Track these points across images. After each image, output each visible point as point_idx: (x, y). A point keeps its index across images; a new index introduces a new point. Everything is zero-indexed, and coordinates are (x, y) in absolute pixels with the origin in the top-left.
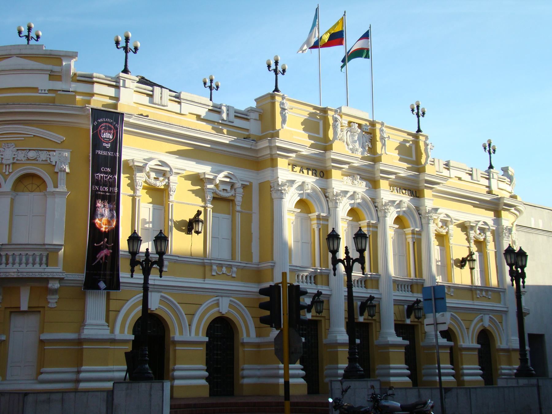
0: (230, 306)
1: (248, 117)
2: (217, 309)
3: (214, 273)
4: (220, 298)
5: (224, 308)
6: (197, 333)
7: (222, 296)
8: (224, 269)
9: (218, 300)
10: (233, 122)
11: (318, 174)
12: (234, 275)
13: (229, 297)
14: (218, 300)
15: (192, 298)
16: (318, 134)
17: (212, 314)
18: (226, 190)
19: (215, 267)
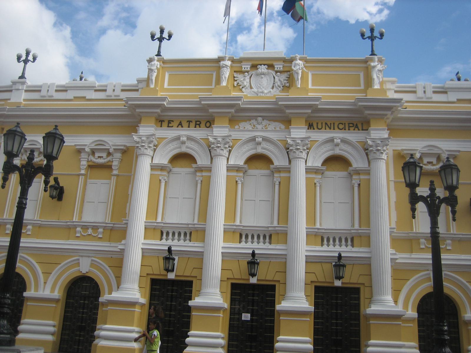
0: (92, 265)
1: (137, 88)
2: (78, 268)
3: (78, 235)
4: (81, 258)
5: (85, 267)
6: (53, 290)
7: (82, 256)
8: (90, 231)
9: (79, 260)
10: (119, 96)
11: (203, 125)
12: (100, 236)
13: (89, 257)
14: (79, 260)
15: (50, 258)
16: (211, 85)
17: (72, 273)
18: (103, 157)
19: (79, 229)
